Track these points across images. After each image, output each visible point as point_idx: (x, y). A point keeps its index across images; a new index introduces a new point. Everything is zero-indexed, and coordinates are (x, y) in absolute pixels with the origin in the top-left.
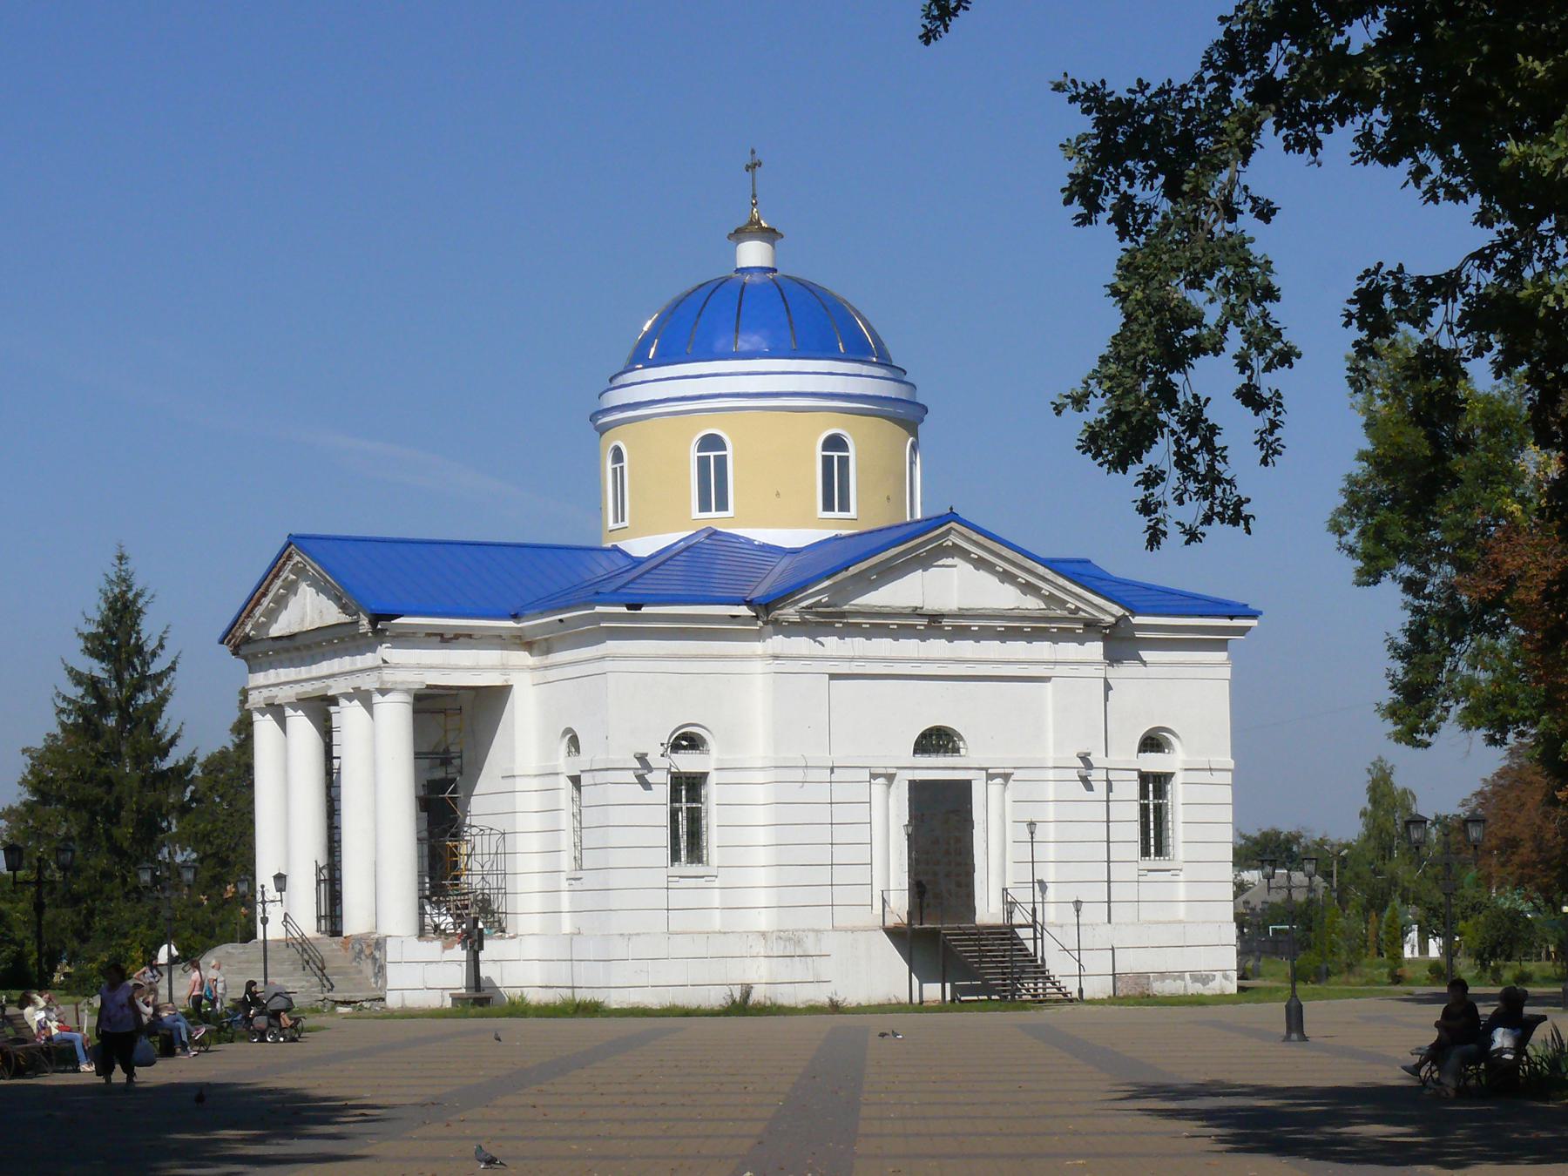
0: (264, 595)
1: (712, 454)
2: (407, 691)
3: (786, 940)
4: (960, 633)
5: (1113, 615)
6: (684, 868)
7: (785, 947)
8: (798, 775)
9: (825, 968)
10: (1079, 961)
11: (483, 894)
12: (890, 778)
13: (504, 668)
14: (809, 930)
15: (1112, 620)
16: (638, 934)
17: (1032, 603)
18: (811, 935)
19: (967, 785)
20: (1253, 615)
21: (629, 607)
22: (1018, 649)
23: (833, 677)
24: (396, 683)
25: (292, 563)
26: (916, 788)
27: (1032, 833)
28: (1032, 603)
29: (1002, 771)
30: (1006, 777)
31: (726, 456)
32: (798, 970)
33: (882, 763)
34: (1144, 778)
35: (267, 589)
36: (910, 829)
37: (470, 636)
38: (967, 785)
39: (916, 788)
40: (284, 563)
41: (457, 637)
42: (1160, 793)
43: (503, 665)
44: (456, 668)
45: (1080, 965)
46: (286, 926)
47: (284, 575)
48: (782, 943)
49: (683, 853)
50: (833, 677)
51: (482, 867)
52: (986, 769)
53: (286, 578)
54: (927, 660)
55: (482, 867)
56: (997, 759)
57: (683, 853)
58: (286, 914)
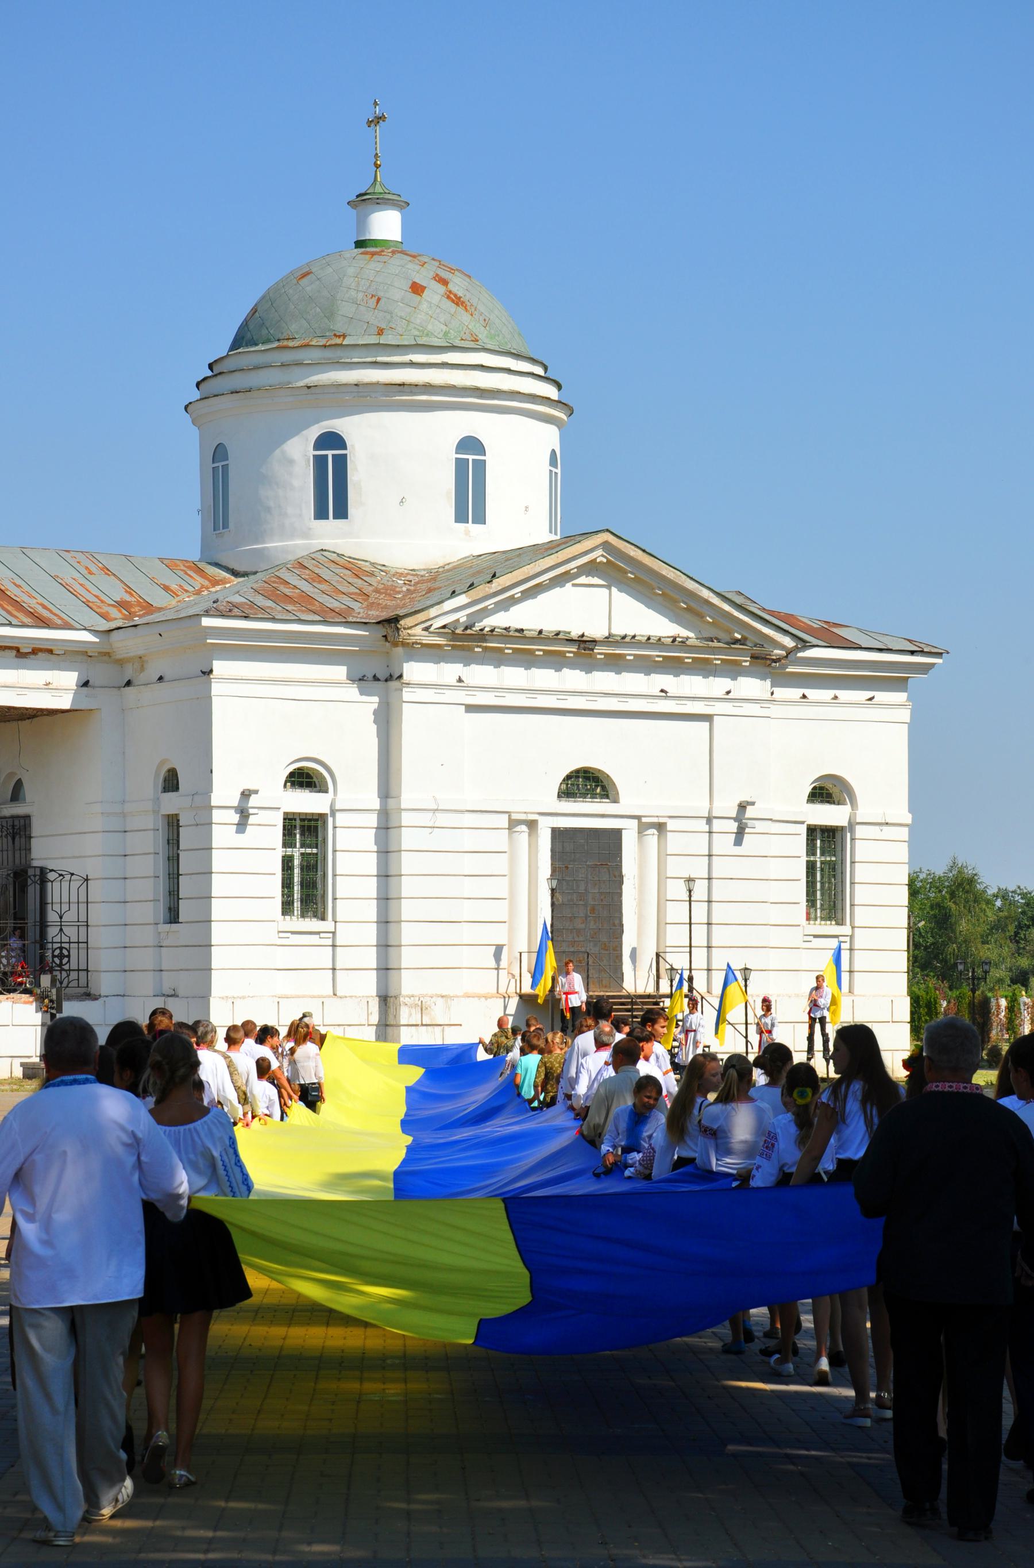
1: (330, 453)
3: (411, 1007)
4: (616, 664)
6: (296, 923)
10: (746, 1037)
11: (61, 948)
12: (532, 825)
16: (244, 998)
19: (616, 835)
23: (471, 708)
26: (559, 835)
27: (690, 891)
29: (655, 820)
30: (660, 827)
33: (522, 808)
34: (812, 830)
36: (555, 883)
38: (616, 835)
39: (559, 835)
45: (747, 1042)
49: (297, 905)
50: (471, 708)
51: (61, 917)
52: (638, 818)
55: (61, 917)
56: (652, 808)
57: (297, 905)
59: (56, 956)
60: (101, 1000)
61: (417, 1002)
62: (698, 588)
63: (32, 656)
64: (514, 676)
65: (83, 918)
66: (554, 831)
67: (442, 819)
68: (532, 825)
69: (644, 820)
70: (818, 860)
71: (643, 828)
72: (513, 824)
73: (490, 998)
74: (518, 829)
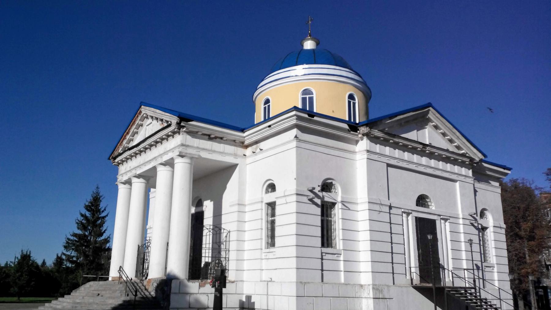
0: (128, 133)
5: (479, 158)
13: (235, 155)
20: (509, 169)
21: (309, 115)
22: (449, 167)
24: (187, 153)
25: (141, 116)
31: (313, 97)
35: (129, 131)
37: (221, 138)
40: (138, 117)
41: (216, 138)
43: (235, 154)
44: (214, 152)
46: (120, 273)
47: (137, 122)
53: (138, 124)
58: (121, 267)
59: (217, 263)
60: (235, 283)
63: (214, 139)
65: (227, 248)
66: (416, 218)
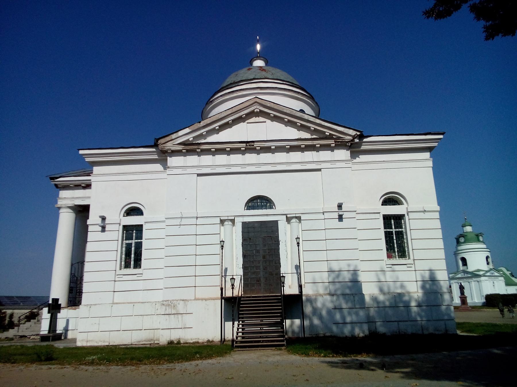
2: (70, 207)
3: (166, 306)
4: (267, 150)
7: (166, 310)
8: (178, 222)
9: (188, 320)
14: (181, 300)
15: (351, 138)
17: (308, 136)
18: (182, 302)
19: (276, 222)
23: (199, 175)
26: (245, 225)
28: (308, 136)
30: (299, 218)
32: (173, 322)
33: (225, 214)
34: (387, 219)
38: (276, 222)
39: (245, 225)
42: (399, 225)
48: (164, 307)
50: (199, 175)
54: (249, 165)
56: (292, 210)
61: (169, 303)
62: (302, 115)
64: (221, 159)
67: (184, 221)
68: (233, 221)
69: (288, 216)
70: (394, 230)
71: (289, 220)
72: (222, 222)
73: (208, 300)
74: (226, 223)
